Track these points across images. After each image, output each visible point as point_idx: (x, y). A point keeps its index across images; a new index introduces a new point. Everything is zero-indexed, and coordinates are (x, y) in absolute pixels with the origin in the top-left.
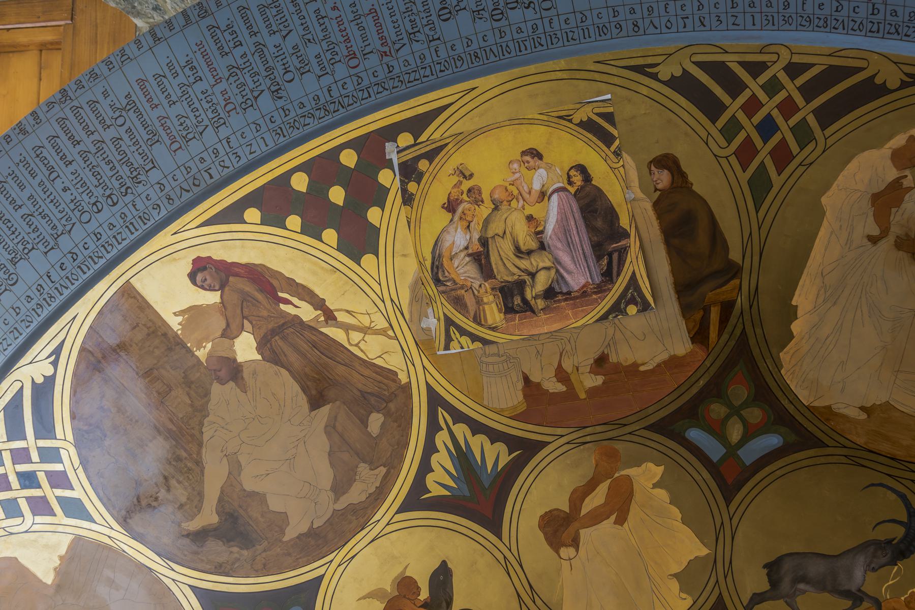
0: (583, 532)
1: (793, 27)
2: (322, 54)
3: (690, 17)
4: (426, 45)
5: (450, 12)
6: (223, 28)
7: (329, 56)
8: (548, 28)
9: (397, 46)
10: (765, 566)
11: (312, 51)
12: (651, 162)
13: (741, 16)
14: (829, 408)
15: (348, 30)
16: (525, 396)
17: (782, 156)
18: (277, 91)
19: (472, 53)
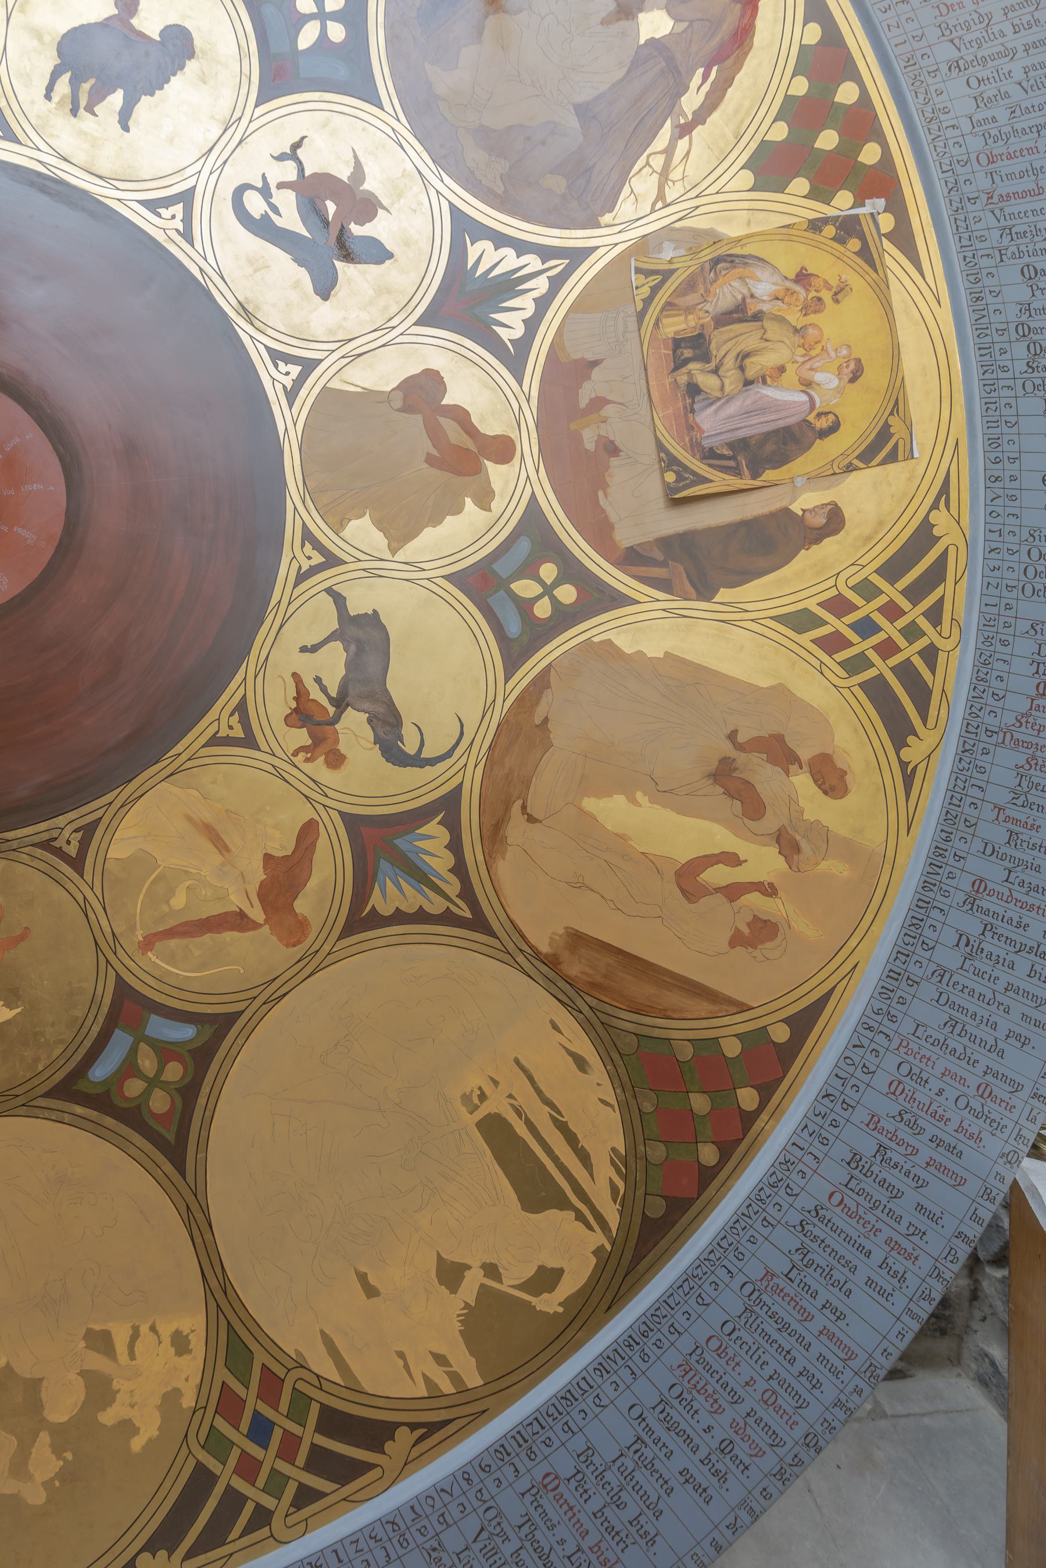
0: (419, 418)
1: (980, 645)
2: (996, 124)
3: (1001, 539)
4: (995, 245)
5: (1030, 278)
6: (1037, 15)
7: (993, 132)
8: (1002, 383)
9: (997, 212)
10: (374, 611)
11: (1002, 114)
12: (836, 505)
13: (997, 592)
14: (548, 686)
15: (1021, 159)
16: (576, 361)
17: (832, 644)
18: (958, 66)
19: (982, 295)
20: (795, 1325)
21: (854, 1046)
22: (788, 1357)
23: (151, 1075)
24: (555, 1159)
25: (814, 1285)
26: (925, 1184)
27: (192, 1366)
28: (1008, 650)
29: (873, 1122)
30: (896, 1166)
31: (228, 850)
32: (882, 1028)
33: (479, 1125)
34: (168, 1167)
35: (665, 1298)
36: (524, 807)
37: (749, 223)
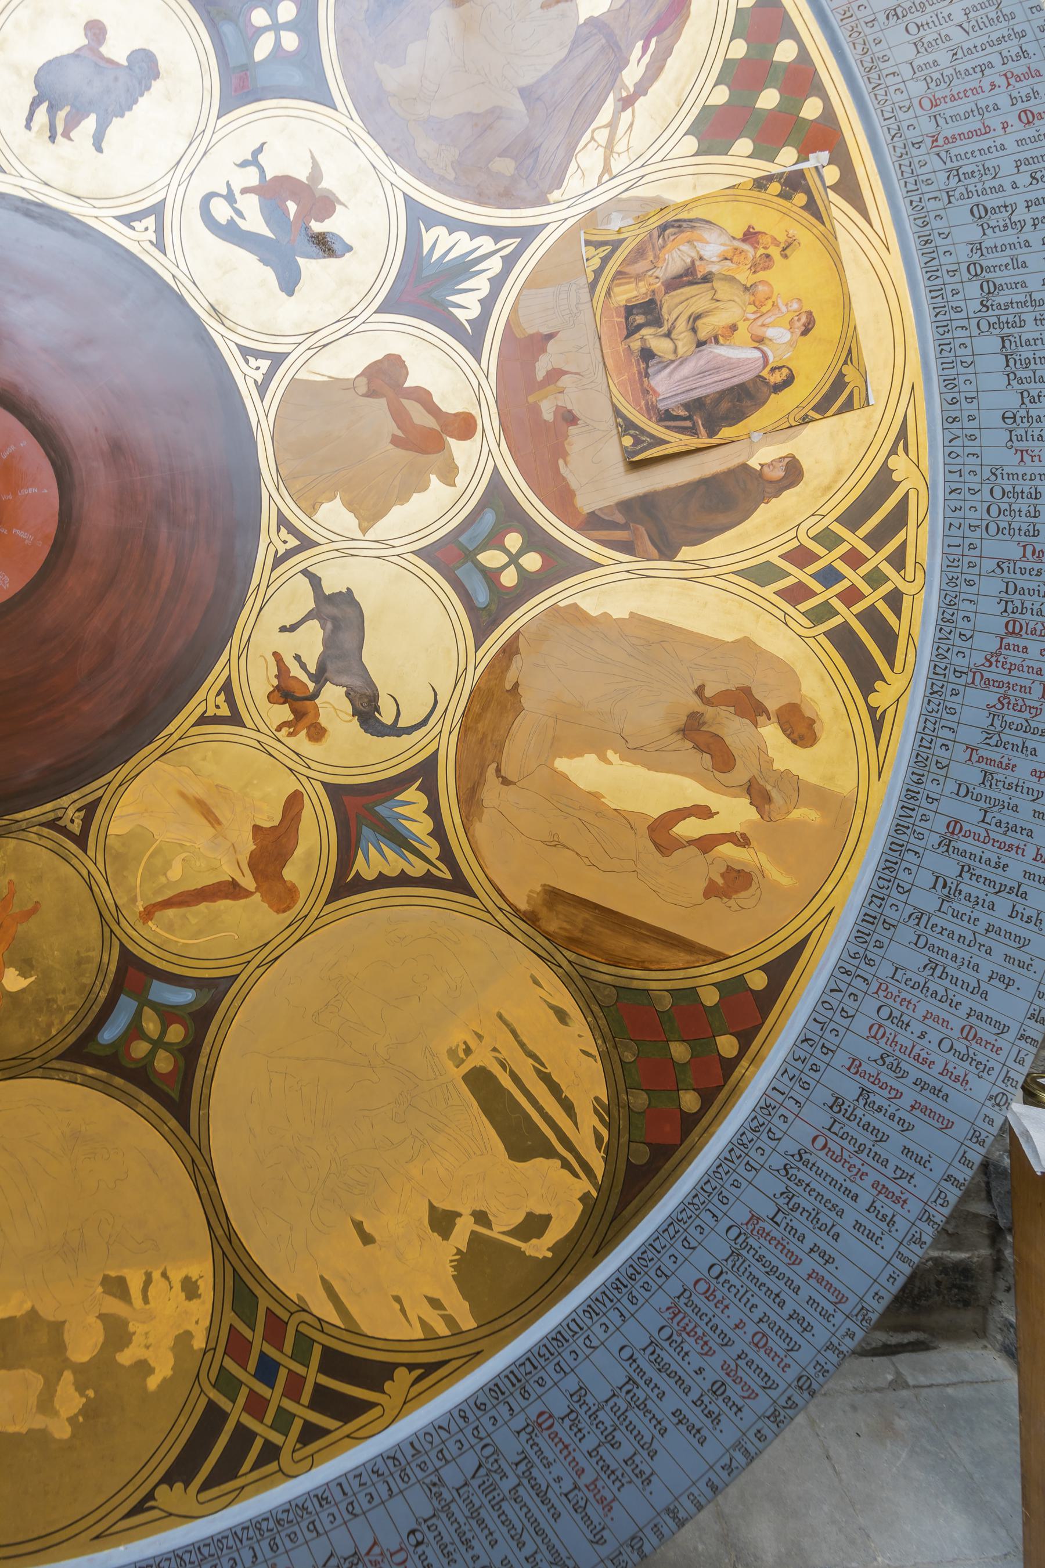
0: (383, 401)
2: (938, 68)
4: (943, 187)
5: (980, 217)
7: (935, 76)
8: (955, 324)
9: (943, 155)
10: (348, 589)
11: (943, 58)
12: (794, 457)
13: (960, 533)
14: (517, 652)
15: (965, 100)
16: (532, 336)
17: (796, 594)
18: (896, 14)
20: (783, 1269)
21: (832, 991)
22: (777, 1300)
23: (155, 1037)
24: (540, 1110)
26: (911, 1127)
27: (201, 1310)
28: (974, 589)
29: (855, 1066)
30: (880, 1109)
31: (219, 823)
32: (859, 972)
33: (466, 1078)
34: (173, 1123)
35: (651, 1241)
36: (498, 770)
37: (695, 187)
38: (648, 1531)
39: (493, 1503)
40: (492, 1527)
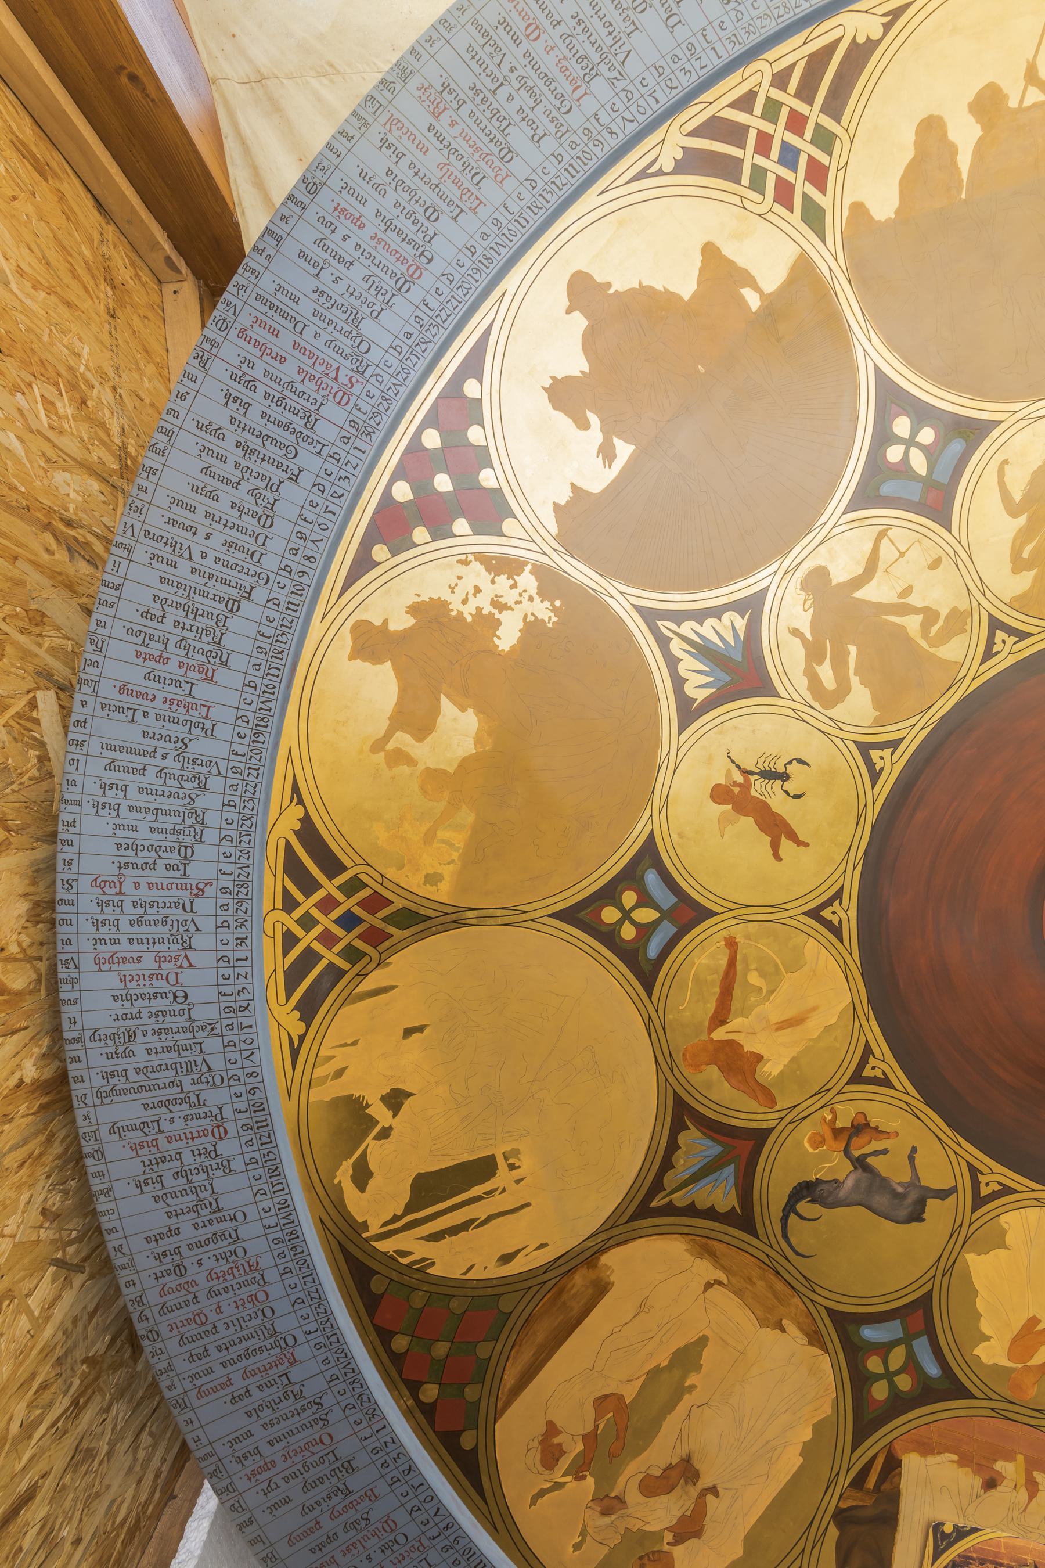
10: (924, 1220)
14: (810, 1344)
20: (245, 1362)
21: (438, 1509)
22: (223, 1347)
25: (267, 1391)
26: (303, 1513)
27: (414, 882)
29: (372, 1496)
30: (329, 1497)
31: (777, 1029)
32: (442, 1537)
33: (492, 1157)
35: (314, 1275)
36: (720, 1283)
38: (103, 1167)
39: (178, 1065)
40: (161, 1056)
